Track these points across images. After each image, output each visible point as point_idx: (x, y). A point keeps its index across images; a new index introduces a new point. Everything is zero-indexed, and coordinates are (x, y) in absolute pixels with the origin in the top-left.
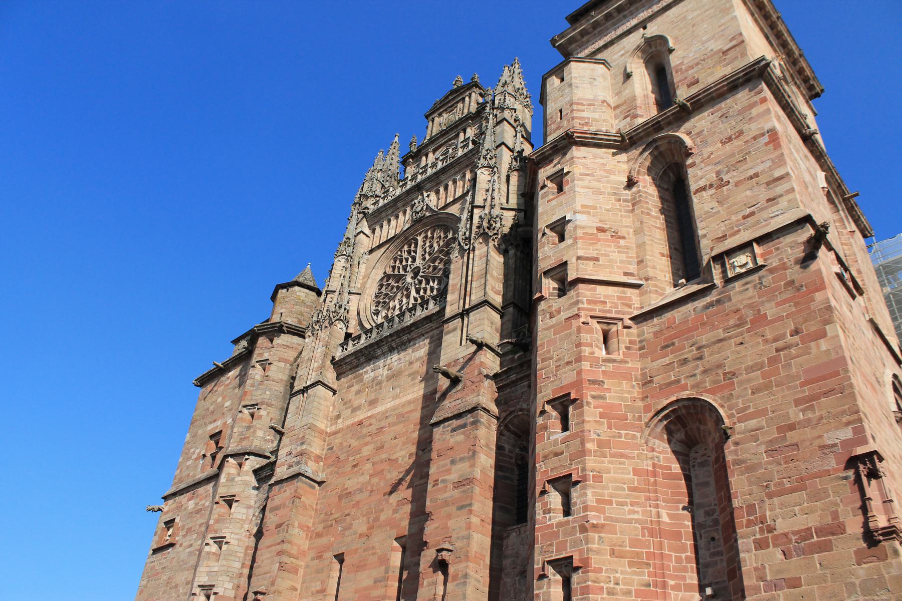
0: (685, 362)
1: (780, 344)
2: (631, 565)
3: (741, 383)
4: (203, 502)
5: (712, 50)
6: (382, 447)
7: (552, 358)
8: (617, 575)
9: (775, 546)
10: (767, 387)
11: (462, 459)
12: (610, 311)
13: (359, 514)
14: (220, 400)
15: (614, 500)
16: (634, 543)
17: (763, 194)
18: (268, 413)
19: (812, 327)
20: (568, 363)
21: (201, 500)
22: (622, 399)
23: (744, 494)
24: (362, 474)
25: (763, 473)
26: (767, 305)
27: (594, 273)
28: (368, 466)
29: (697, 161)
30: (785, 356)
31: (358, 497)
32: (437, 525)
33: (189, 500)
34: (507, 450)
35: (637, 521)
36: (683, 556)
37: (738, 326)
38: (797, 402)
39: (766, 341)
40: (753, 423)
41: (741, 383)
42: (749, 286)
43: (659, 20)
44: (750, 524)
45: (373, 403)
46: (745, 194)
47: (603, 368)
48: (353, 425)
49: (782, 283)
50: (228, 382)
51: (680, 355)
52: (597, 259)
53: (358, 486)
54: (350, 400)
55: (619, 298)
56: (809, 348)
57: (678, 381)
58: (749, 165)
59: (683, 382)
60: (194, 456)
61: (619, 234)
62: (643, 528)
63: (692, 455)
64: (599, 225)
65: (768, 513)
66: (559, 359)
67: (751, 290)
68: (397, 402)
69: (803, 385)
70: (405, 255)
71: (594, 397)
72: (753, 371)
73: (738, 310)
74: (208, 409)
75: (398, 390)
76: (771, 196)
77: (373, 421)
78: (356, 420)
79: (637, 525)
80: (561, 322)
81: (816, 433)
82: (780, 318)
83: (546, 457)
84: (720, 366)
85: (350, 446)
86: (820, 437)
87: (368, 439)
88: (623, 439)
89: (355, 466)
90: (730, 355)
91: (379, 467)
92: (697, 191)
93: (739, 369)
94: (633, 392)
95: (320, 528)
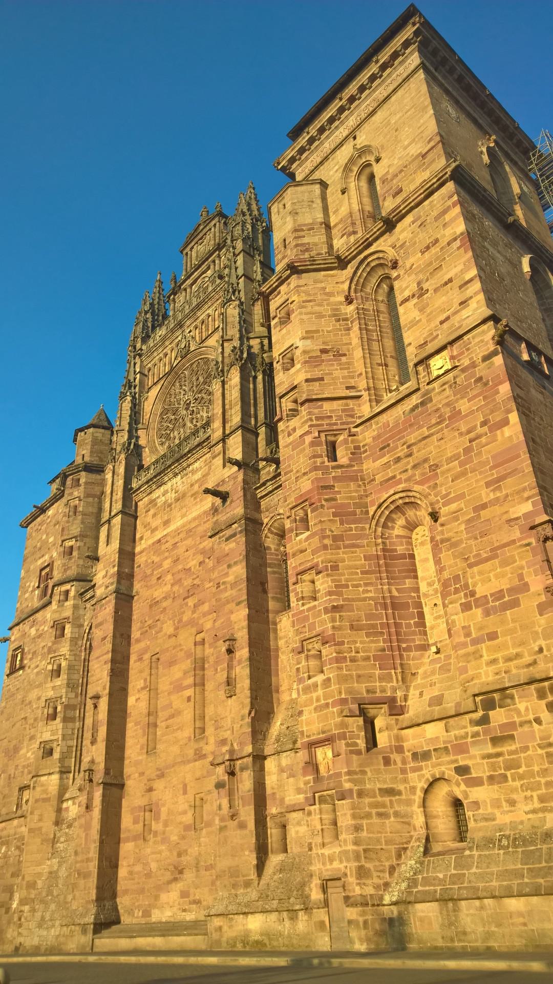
0: (398, 460)
1: (472, 435)
2: (368, 635)
3: (443, 473)
4: (43, 627)
5: (412, 155)
6: (178, 559)
7: (292, 471)
8: (358, 645)
9: (476, 607)
10: (464, 474)
11: (236, 563)
12: (336, 424)
13: (166, 619)
14: (44, 537)
15: (350, 583)
16: (369, 617)
18: (85, 543)
19: (497, 417)
20: (305, 474)
21: (40, 626)
22: (351, 498)
23: (450, 566)
24: (166, 584)
25: (464, 548)
26: (461, 402)
27: (320, 392)
28: (169, 577)
31: (165, 604)
32: (222, 620)
33: (31, 627)
34: (273, 549)
35: (370, 598)
36: (412, 622)
37: (438, 423)
38: (488, 485)
39: (461, 434)
40: (454, 506)
41: (443, 473)
42: (446, 386)
43: (366, 127)
44: (457, 591)
45: (166, 523)
46: (440, 300)
47: (333, 474)
48: (153, 544)
49: (473, 380)
50: (49, 520)
51: (395, 454)
52: (322, 379)
53: (164, 596)
55: (343, 411)
56: (496, 435)
57: (394, 477)
59: (398, 477)
60: (31, 589)
61: (340, 352)
62: (376, 604)
63: (414, 536)
64: (322, 347)
65: (470, 581)
66: (297, 472)
67: (448, 390)
68: (185, 519)
69: (491, 468)
71: (326, 500)
72: (452, 462)
73: (437, 410)
74: (35, 547)
75: (184, 510)
76: (463, 300)
77: (169, 538)
79: (371, 602)
80: (297, 439)
81: (503, 509)
82: (472, 412)
83: (294, 555)
84: (426, 460)
86: (507, 512)
87: (167, 554)
88: (354, 532)
89: (159, 578)
90: (431, 449)
91: (178, 577)
93: (441, 461)
94: (360, 491)
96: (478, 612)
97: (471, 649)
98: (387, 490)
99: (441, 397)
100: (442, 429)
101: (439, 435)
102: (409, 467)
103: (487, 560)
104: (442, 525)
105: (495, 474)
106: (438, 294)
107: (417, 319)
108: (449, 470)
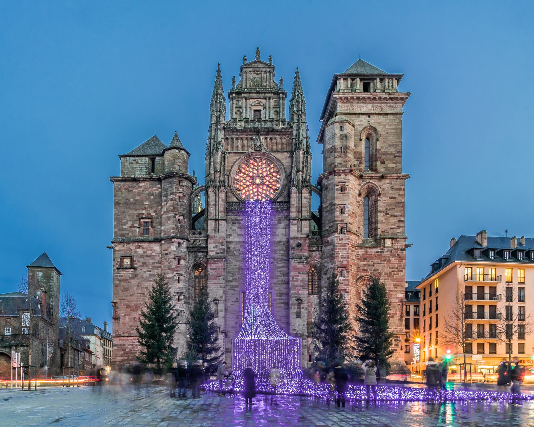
0: (369, 265)
1: (393, 270)
10: (388, 279)
29: (381, 200)
30: (394, 273)
37: (384, 261)
39: (390, 268)
41: (382, 276)
46: (393, 220)
54: (236, 230)
73: (385, 257)
84: (378, 270)
85: (240, 250)
90: (380, 267)
95: (231, 279)
99: (387, 254)
100: (385, 263)
101: (384, 265)
102: (373, 269)
105: (396, 283)
107: (384, 221)
108: (384, 276)
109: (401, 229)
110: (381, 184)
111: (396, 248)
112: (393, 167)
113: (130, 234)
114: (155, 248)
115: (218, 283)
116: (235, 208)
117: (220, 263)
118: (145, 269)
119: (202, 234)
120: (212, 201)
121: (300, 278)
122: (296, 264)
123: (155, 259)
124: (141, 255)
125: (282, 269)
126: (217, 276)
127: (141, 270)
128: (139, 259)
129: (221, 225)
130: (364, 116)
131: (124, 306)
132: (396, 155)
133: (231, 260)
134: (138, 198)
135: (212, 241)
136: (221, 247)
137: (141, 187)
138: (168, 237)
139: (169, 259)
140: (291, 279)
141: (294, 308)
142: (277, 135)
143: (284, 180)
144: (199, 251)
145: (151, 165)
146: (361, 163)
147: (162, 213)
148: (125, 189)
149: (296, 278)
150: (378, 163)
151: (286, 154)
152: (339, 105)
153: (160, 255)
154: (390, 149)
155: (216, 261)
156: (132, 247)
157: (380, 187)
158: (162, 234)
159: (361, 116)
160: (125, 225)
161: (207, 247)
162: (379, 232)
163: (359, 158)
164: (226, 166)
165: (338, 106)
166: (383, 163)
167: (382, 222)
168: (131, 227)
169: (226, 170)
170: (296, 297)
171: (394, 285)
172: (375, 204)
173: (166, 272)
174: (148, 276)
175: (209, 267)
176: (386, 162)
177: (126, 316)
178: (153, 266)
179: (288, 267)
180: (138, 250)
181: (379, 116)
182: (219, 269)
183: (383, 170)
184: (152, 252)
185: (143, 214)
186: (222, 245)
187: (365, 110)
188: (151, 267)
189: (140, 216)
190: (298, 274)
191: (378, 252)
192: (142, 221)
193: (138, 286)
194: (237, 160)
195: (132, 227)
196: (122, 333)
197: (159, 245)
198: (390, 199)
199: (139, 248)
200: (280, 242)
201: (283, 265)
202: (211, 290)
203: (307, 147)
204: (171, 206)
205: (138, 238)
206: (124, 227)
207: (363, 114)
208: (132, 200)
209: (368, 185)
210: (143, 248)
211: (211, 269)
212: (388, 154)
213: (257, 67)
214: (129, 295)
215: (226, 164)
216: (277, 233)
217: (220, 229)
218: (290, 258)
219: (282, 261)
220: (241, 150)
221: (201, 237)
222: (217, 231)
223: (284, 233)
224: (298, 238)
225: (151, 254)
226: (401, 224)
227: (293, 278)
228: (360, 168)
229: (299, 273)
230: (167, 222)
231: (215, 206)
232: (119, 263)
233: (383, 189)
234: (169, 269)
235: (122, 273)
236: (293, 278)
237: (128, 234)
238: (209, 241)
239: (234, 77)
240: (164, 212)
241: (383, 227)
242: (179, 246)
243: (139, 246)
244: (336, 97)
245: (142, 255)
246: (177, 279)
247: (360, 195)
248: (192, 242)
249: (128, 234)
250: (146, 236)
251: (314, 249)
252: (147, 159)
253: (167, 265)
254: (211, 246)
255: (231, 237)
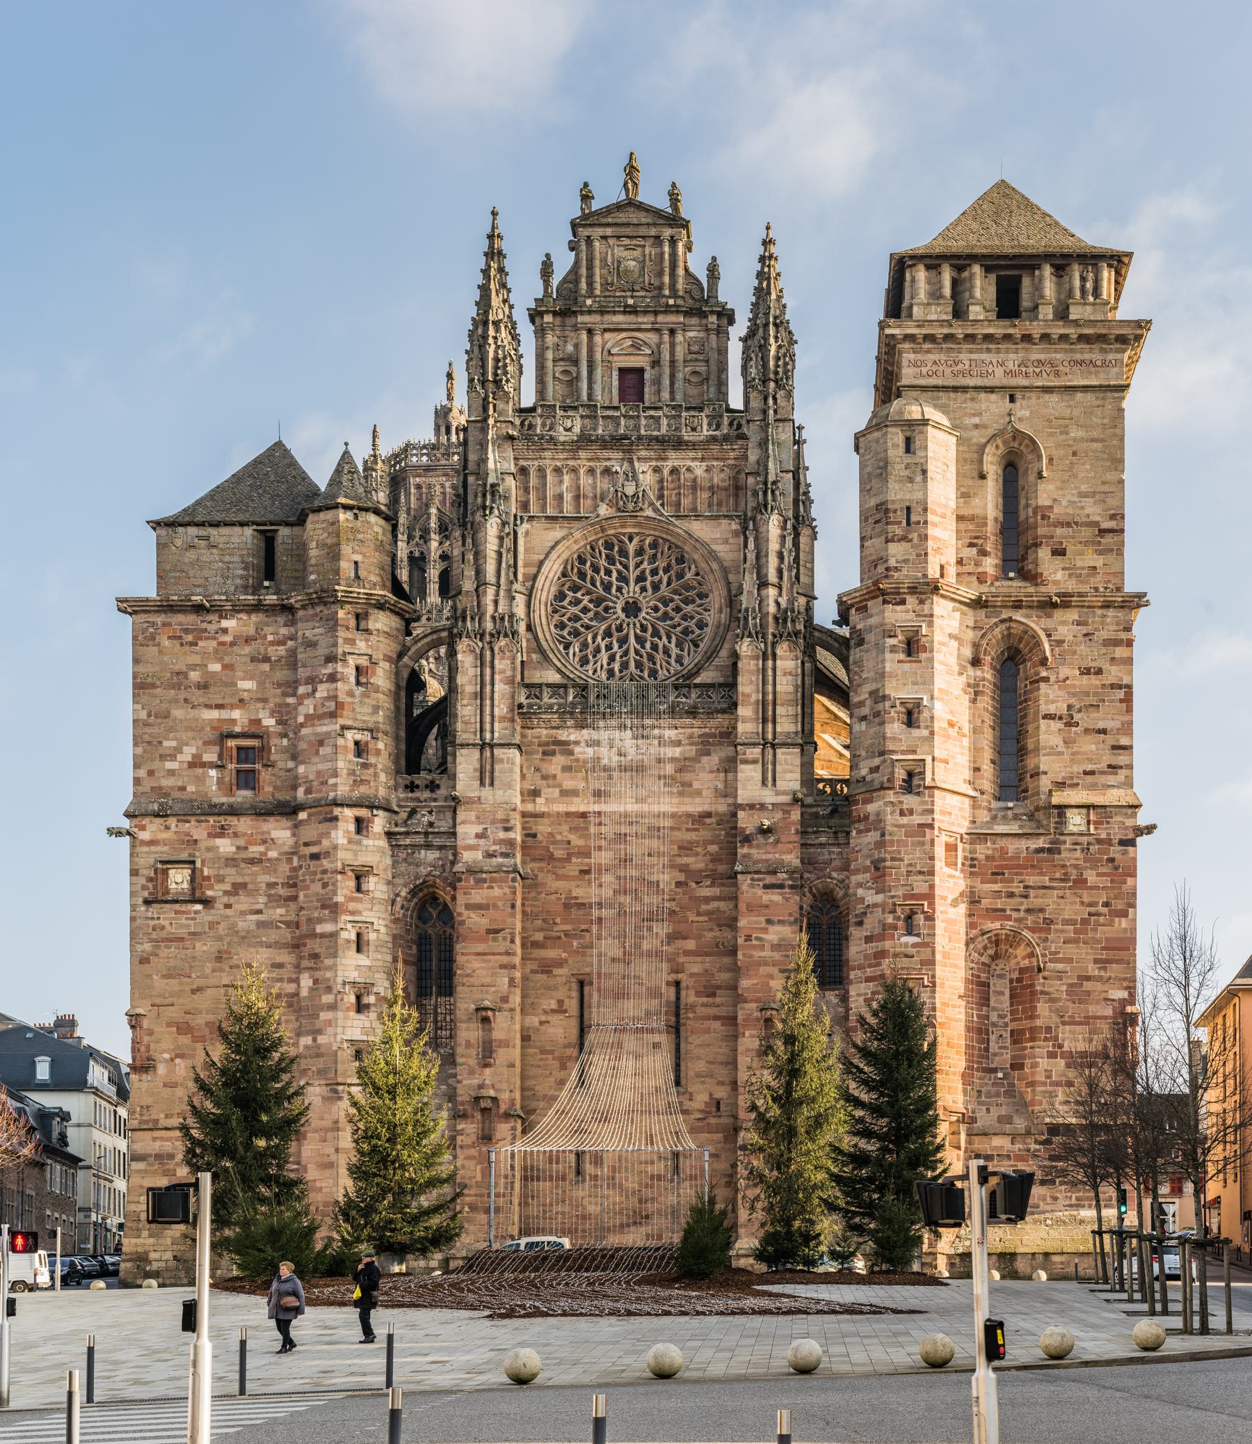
1: (1093, 909)
10: (1076, 941)
17: (1108, 758)
19: (1119, 905)
26: (1089, 871)
29: (1053, 679)
39: (1082, 903)
40: (1060, 966)
41: (1057, 931)
42: (1078, 847)
44: (1046, 1039)
45: (598, 794)
46: (1089, 745)
54: (554, 777)
58: (1100, 715)
68: (645, 808)
69: (1103, 949)
70: (603, 563)
73: (1064, 866)
76: (1113, 763)
78: (573, 809)
82: (1097, 888)
84: (1041, 910)
85: (569, 843)
90: (1050, 901)
92: (1046, 717)
95: (539, 936)
96: (1062, 1063)
97: (1049, 1088)
98: (993, 920)
99: (1070, 856)
100: (1064, 888)
101: (1061, 893)
102: (1023, 908)
103: (1080, 1023)
104: (1045, 978)
105: (1104, 955)
106: (1089, 737)
107: (1059, 749)
108: (1062, 931)
109: (1122, 775)
110: (1047, 623)
111: (1103, 836)
112: (1095, 568)
113: (191, 788)
114: (275, 834)
115: (494, 954)
116: (551, 706)
117: (501, 887)
118: (242, 902)
119: (438, 787)
120: (467, 679)
121: (774, 934)
122: (760, 892)
123: (275, 871)
124: (227, 859)
125: (714, 905)
126: (489, 931)
127: (228, 906)
128: (221, 872)
129: (502, 761)
130: (993, 397)
131: (169, 1025)
132: (1107, 525)
133: (540, 876)
134: (215, 667)
135: (472, 816)
136: (502, 835)
137: (225, 631)
138: (320, 800)
139: (325, 872)
140: (740, 941)
141: (752, 1036)
142: (694, 459)
143: (721, 612)
144: (428, 846)
145: (262, 553)
146: (983, 553)
147: (301, 719)
148: (169, 638)
149: (758, 939)
150: (1044, 553)
151: (724, 522)
152: (908, 357)
153: (295, 859)
154: (1082, 508)
155: (485, 881)
156: (197, 830)
157: (1049, 636)
158: (300, 793)
159: (983, 396)
160: (173, 757)
161: (454, 834)
162: (1045, 783)
163: (977, 538)
164: (520, 563)
165: (905, 363)
166: (1059, 552)
167: (1053, 752)
168: (193, 764)
169: (520, 577)
170: (756, 1001)
171: (1096, 961)
172: (1031, 692)
173: (316, 915)
174: (253, 927)
175: (461, 899)
176: (1070, 549)
177: (178, 1061)
178: (269, 896)
179: (735, 899)
180: (218, 841)
181: (1047, 396)
182: (495, 906)
183: (1059, 576)
184: (267, 849)
185: (234, 722)
186: (507, 829)
187: (999, 378)
188: (262, 899)
189: (225, 728)
190: (764, 925)
191: (1040, 850)
192: (231, 743)
193: (219, 959)
194: (557, 543)
195: (196, 763)
196: (162, 1116)
197: (289, 824)
198: (1082, 673)
199: (221, 835)
200: (709, 815)
201: (716, 891)
202: (468, 975)
203: (796, 502)
204: (328, 698)
205: (215, 800)
206: (169, 765)
207: (991, 390)
208: (194, 676)
209: (1009, 628)
210: (236, 835)
211: (468, 907)
212: (1076, 523)
213: (628, 225)
214: (187, 988)
215: (521, 557)
216: (696, 785)
217: (496, 774)
218: (736, 873)
219: (715, 878)
220: (570, 508)
221: (435, 800)
222: (487, 781)
223: (720, 786)
224: (762, 807)
225: (262, 854)
226: (1122, 759)
227: (748, 938)
228: (980, 570)
229: (769, 922)
230: (317, 753)
231: (482, 699)
232: (150, 885)
233: (1060, 642)
234: (324, 907)
235: (166, 916)
236: (748, 938)
237: (183, 789)
238: (461, 815)
239: (548, 256)
240: (307, 716)
241: (1056, 767)
242: (358, 831)
243: (222, 827)
244: (893, 336)
245: (233, 859)
246: (353, 937)
247: (976, 662)
248: (404, 815)
249: (183, 789)
250: (243, 795)
251: (823, 839)
252: (249, 531)
253: (318, 894)
254: (467, 830)
255: (538, 800)
